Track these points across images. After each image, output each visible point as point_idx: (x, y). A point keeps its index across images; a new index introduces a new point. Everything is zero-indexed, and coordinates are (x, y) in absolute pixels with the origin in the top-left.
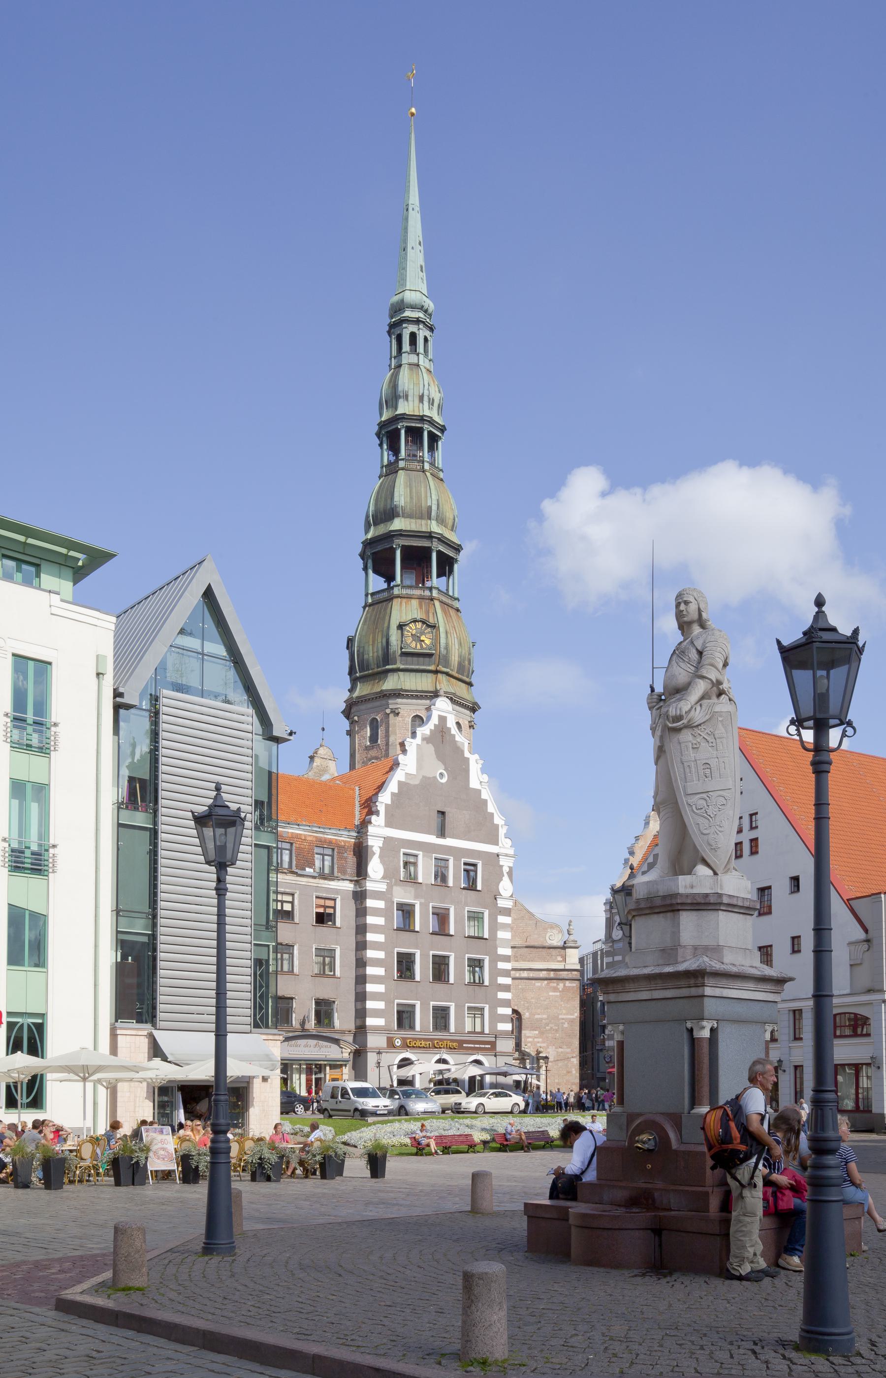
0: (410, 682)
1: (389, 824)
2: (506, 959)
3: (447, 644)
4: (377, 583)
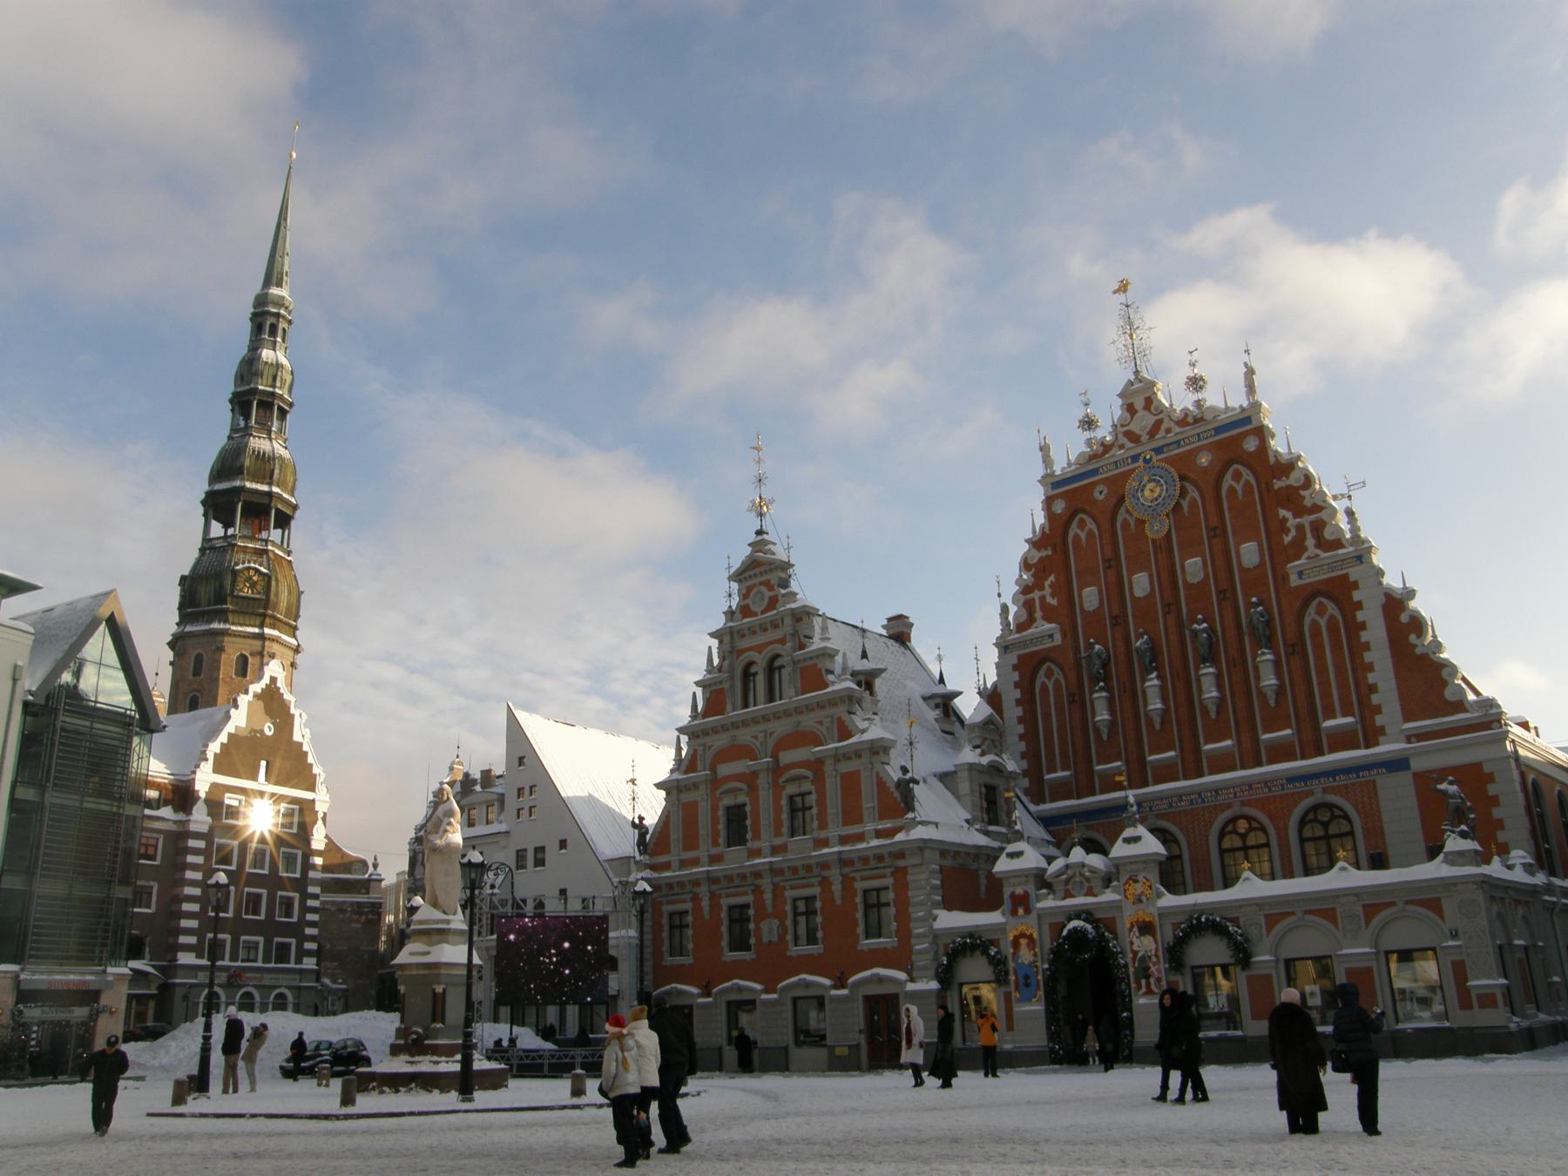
1: (216, 770)
2: (316, 897)
4: (217, 529)
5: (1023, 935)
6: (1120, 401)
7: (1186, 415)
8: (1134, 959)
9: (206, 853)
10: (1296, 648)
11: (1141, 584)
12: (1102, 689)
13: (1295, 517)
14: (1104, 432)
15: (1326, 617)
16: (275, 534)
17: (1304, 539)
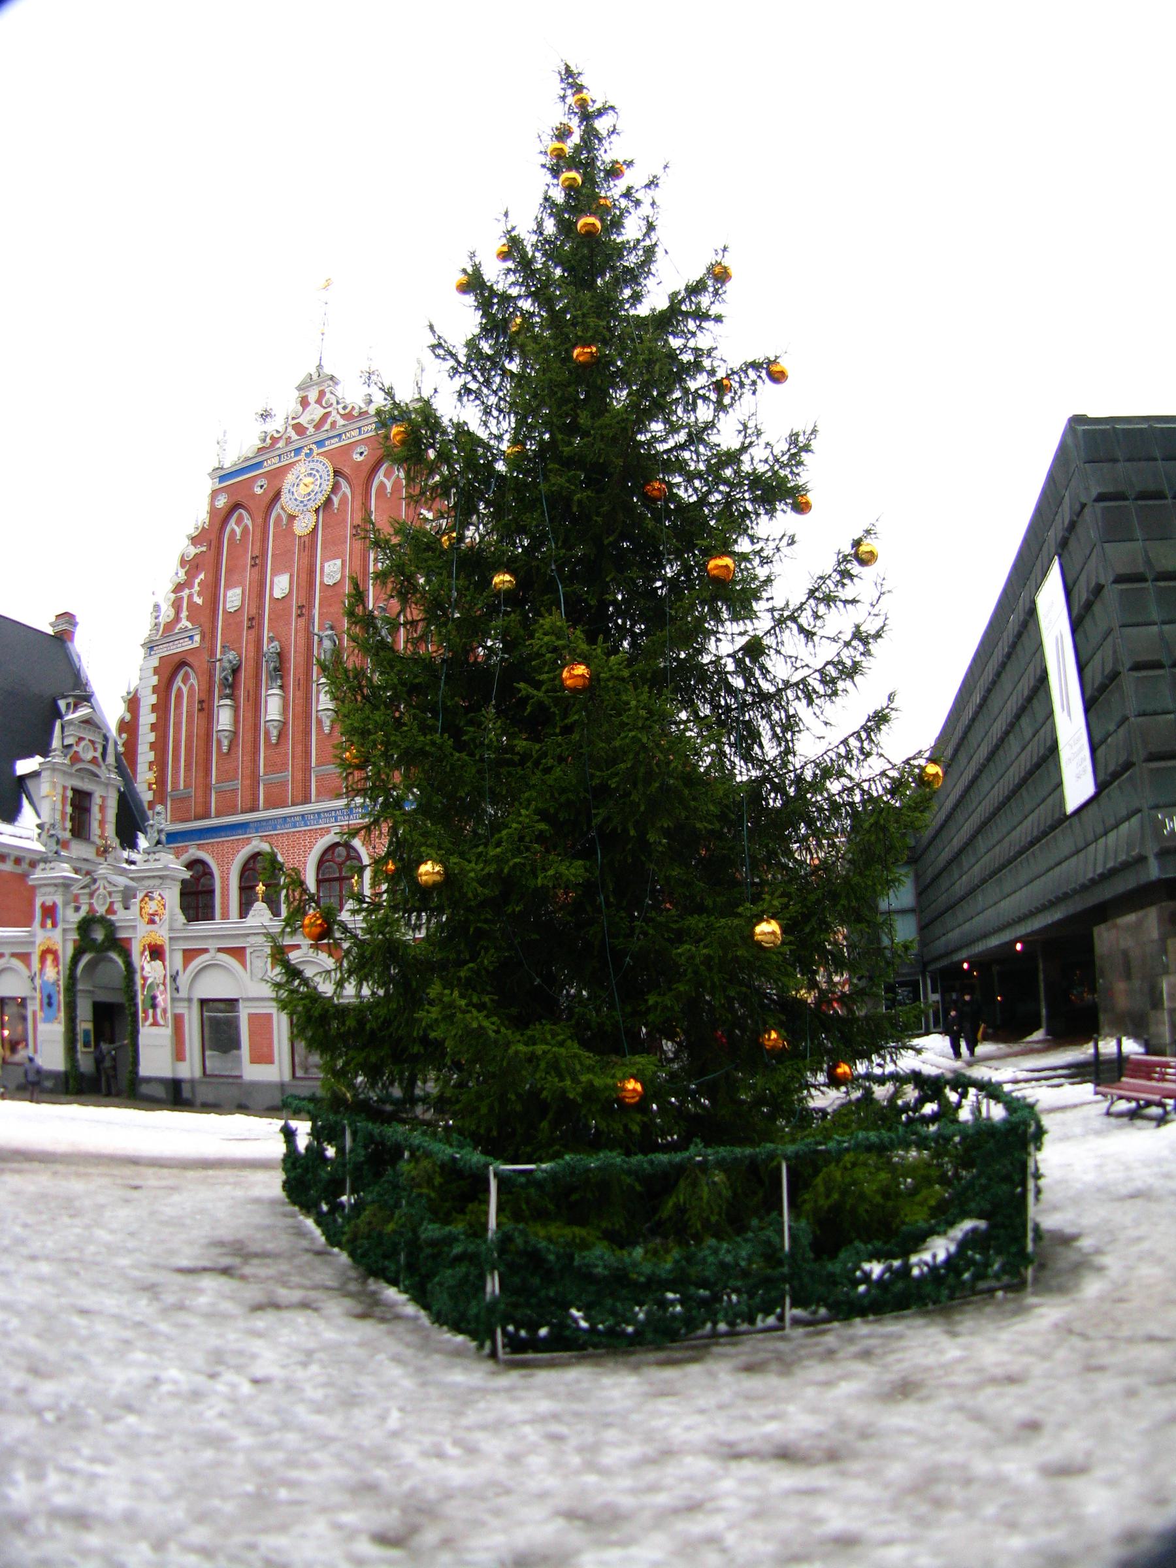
6: (296, 394)
8: (143, 986)
11: (281, 585)
12: (227, 697)
14: (276, 425)
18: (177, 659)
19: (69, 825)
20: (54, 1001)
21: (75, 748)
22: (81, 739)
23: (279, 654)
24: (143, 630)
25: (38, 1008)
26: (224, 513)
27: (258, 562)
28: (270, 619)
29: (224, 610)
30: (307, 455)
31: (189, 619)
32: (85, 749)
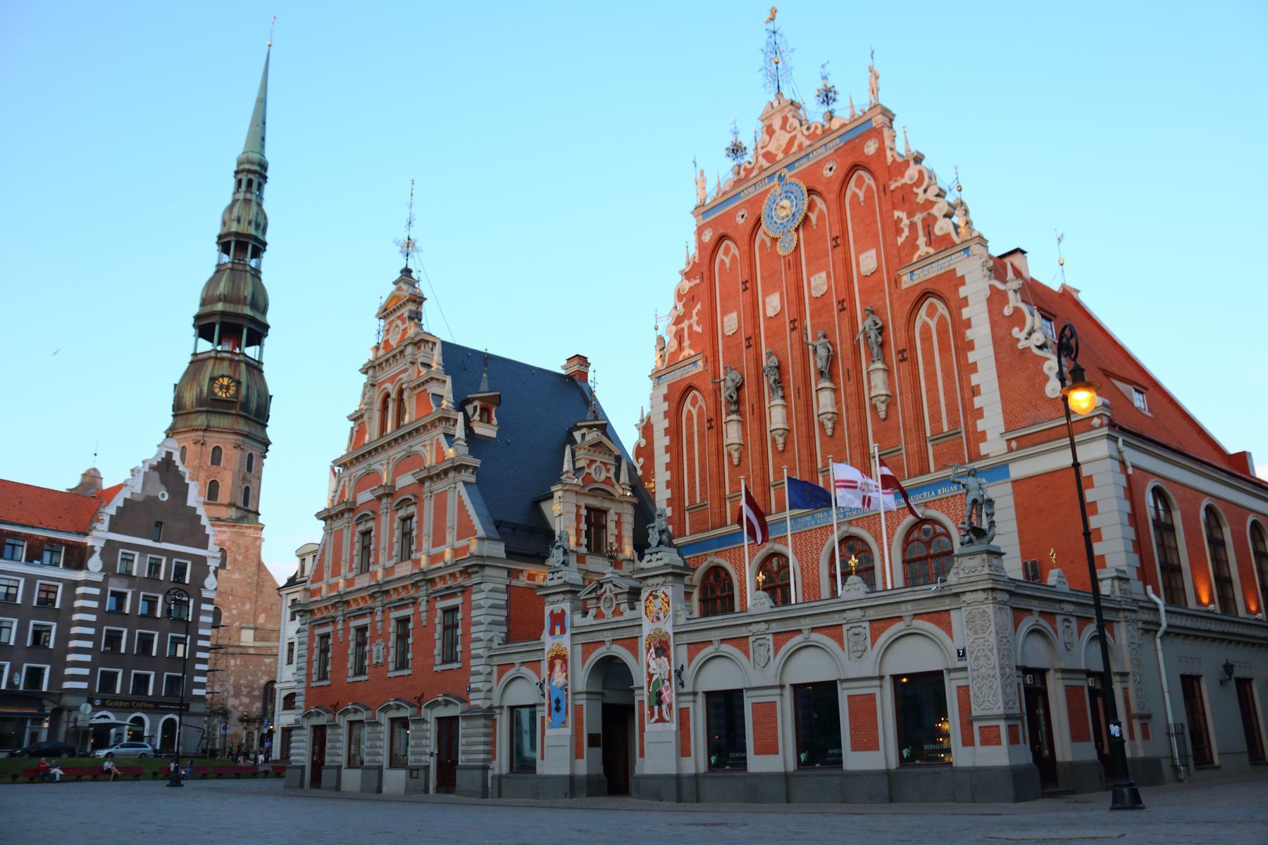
0: (216, 421)
1: (112, 529)
3: (247, 397)
4: (205, 346)
5: (558, 656)
7: (816, 128)
8: (649, 683)
9: (101, 599)
10: (907, 355)
11: (772, 304)
12: (733, 412)
13: (910, 215)
14: (749, 156)
15: (936, 318)
16: (251, 352)
17: (916, 238)
18: (684, 385)
19: (584, 541)
20: (562, 705)
21: (587, 470)
22: (592, 462)
23: (778, 368)
24: (651, 360)
25: (546, 714)
26: (711, 247)
27: (749, 285)
28: (766, 337)
29: (723, 335)
30: (781, 178)
31: (691, 347)
32: (598, 470)
